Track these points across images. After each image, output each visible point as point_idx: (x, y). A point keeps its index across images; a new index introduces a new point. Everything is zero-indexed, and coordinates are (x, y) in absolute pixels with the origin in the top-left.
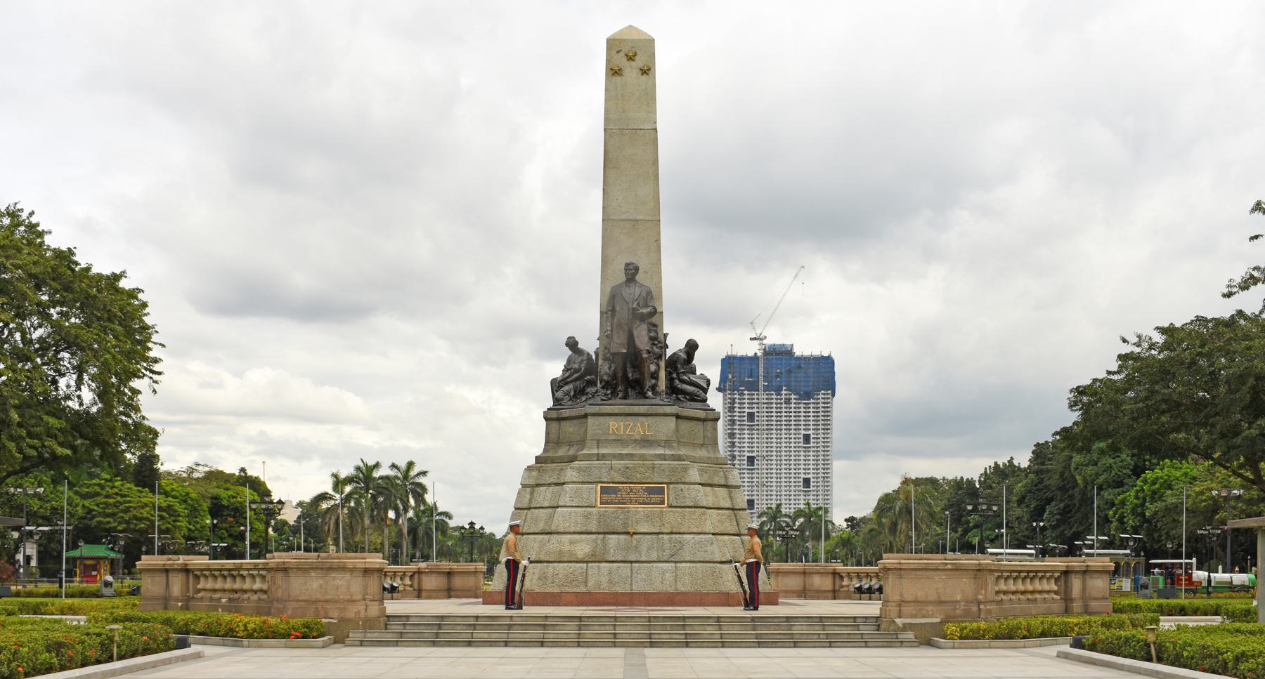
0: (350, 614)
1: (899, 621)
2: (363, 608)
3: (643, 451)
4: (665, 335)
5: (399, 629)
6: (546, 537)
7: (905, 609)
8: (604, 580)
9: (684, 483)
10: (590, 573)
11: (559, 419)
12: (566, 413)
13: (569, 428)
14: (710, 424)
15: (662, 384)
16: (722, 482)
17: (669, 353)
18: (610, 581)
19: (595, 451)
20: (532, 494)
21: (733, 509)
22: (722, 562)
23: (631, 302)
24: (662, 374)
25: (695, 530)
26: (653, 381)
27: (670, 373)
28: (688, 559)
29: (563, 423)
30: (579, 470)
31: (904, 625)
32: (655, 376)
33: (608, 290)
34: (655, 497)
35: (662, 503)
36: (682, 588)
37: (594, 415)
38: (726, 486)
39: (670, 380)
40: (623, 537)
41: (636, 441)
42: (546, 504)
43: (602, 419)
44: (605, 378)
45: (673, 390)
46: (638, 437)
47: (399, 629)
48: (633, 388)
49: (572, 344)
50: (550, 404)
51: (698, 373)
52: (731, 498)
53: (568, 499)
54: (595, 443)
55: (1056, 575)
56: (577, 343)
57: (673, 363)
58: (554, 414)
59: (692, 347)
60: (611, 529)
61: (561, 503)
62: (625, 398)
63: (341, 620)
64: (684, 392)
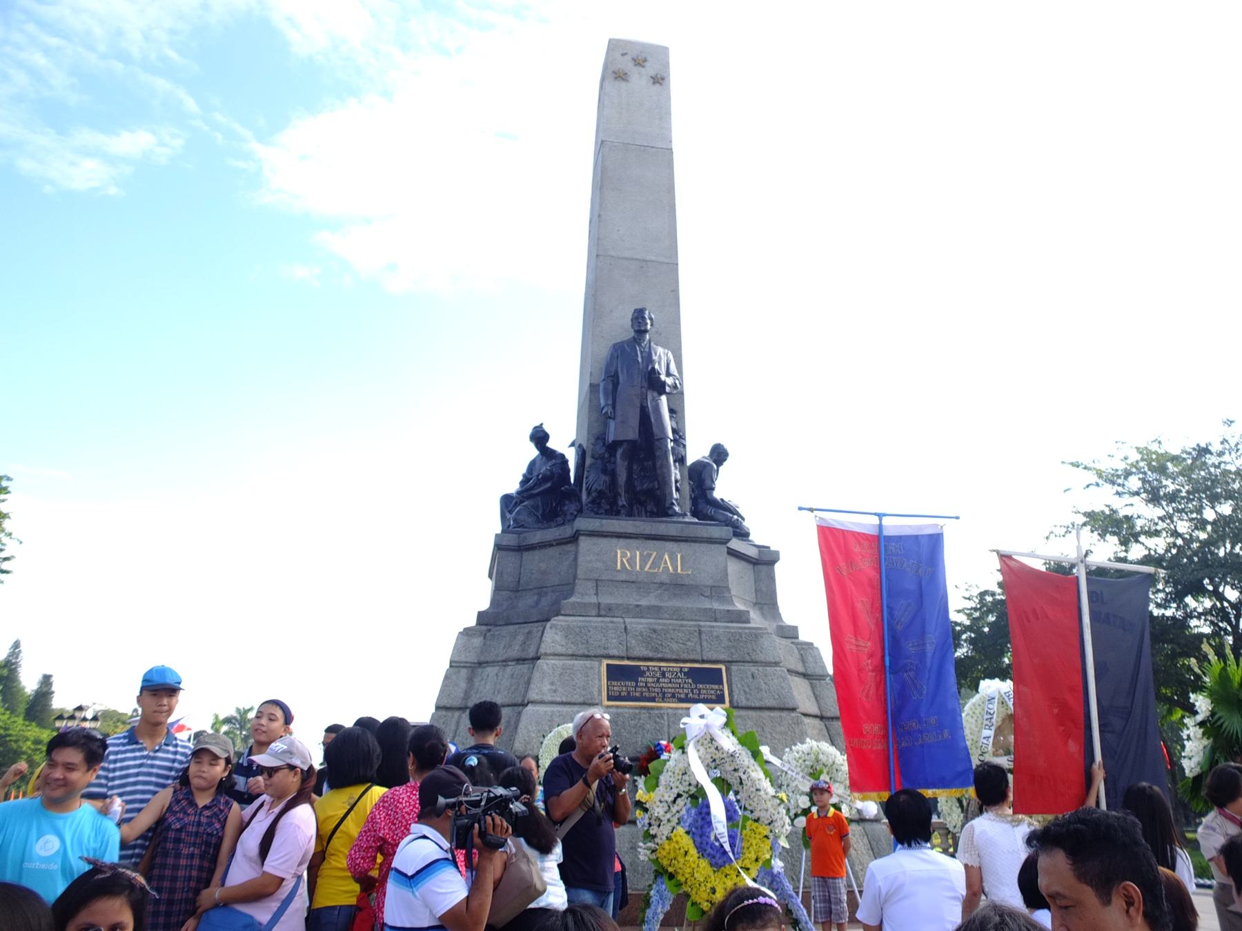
3: (676, 603)
9: (754, 662)
11: (521, 549)
12: (537, 536)
13: (536, 562)
16: (801, 669)
19: (594, 600)
20: (470, 680)
23: (629, 378)
29: (526, 555)
30: (568, 632)
33: (604, 351)
34: (709, 689)
38: (804, 675)
41: (662, 584)
43: (604, 543)
46: (665, 578)
49: (540, 437)
53: (546, 687)
54: (591, 584)
58: (511, 540)
59: (719, 455)
61: (533, 695)
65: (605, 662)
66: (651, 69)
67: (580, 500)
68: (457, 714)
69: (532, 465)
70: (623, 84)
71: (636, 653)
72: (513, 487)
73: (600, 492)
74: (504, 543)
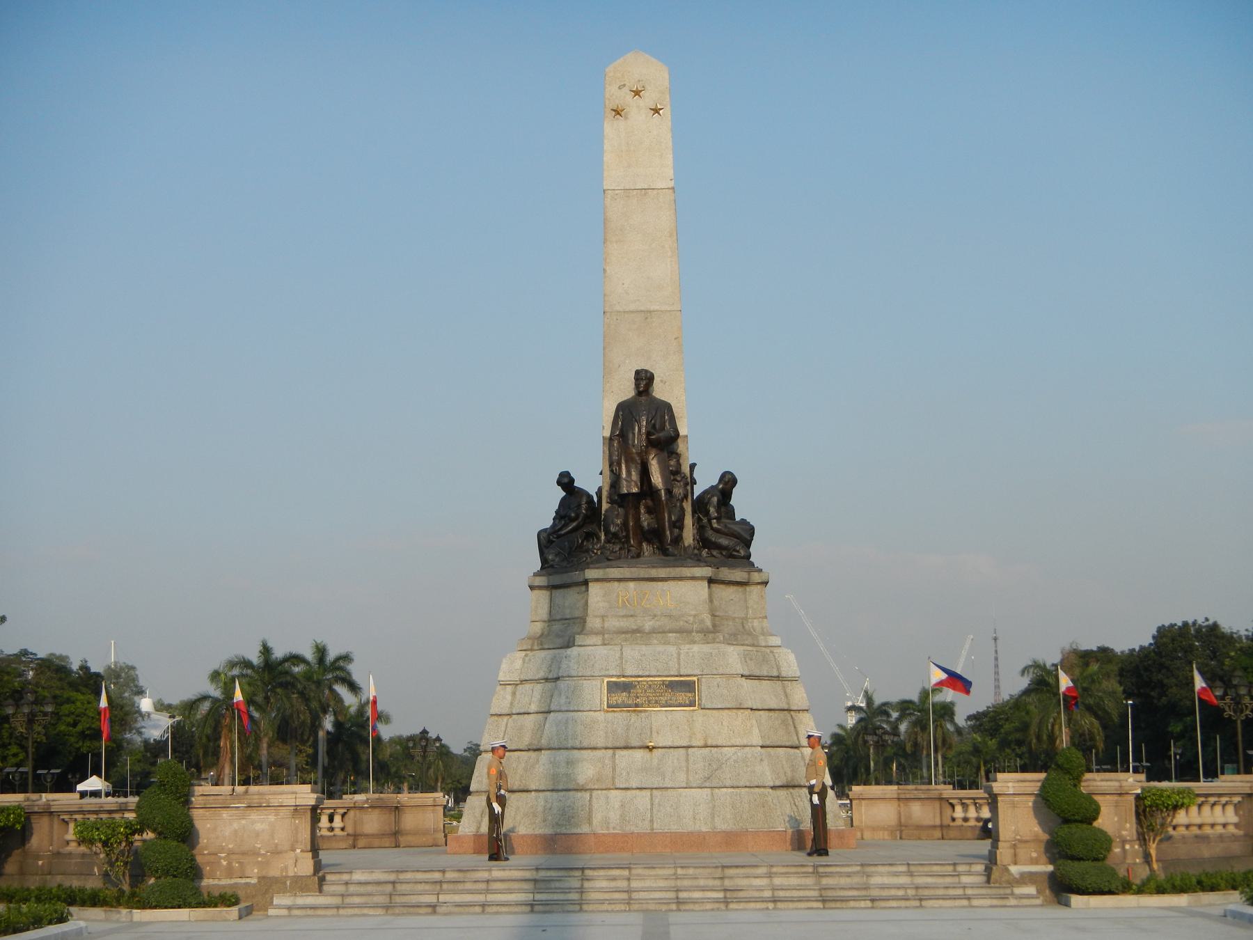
0: (274, 872)
1: (1014, 869)
2: (291, 862)
4: (693, 466)
5: (341, 889)
6: (532, 754)
7: (1022, 852)
8: (614, 817)
10: (595, 806)
14: (755, 590)
15: (689, 535)
16: (775, 674)
17: (698, 490)
18: (623, 817)
20: (514, 694)
21: (789, 710)
22: (772, 788)
24: (689, 521)
25: (738, 742)
26: (676, 531)
27: (699, 519)
28: (728, 783)
31: (1022, 875)
32: (679, 524)
34: (683, 697)
35: (692, 704)
36: (722, 826)
37: (597, 580)
38: (778, 678)
39: (700, 528)
40: (639, 754)
42: (533, 708)
44: (613, 529)
45: (704, 542)
47: (341, 889)
48: (649, 542)
49: (566, 481)
50: (537, 565)
51: (738, 519)
52: (786, 696)
53: (563, 700)
55: (1237, 799)
56: (572, 480)
57: (700, 505)
59: (728, 483)
60: (622, 744)
62: (638, 556)
63: (262, 879)
64: (720, 547)
65: (606, 680)
66: (649, 99)
67: (599, 539)
68: (505, 719)
69: (563, 502)
70: (620, 123)
71: (628, 673)
72: (547, 522)
73: (615, 535)
74: (536, 584)
